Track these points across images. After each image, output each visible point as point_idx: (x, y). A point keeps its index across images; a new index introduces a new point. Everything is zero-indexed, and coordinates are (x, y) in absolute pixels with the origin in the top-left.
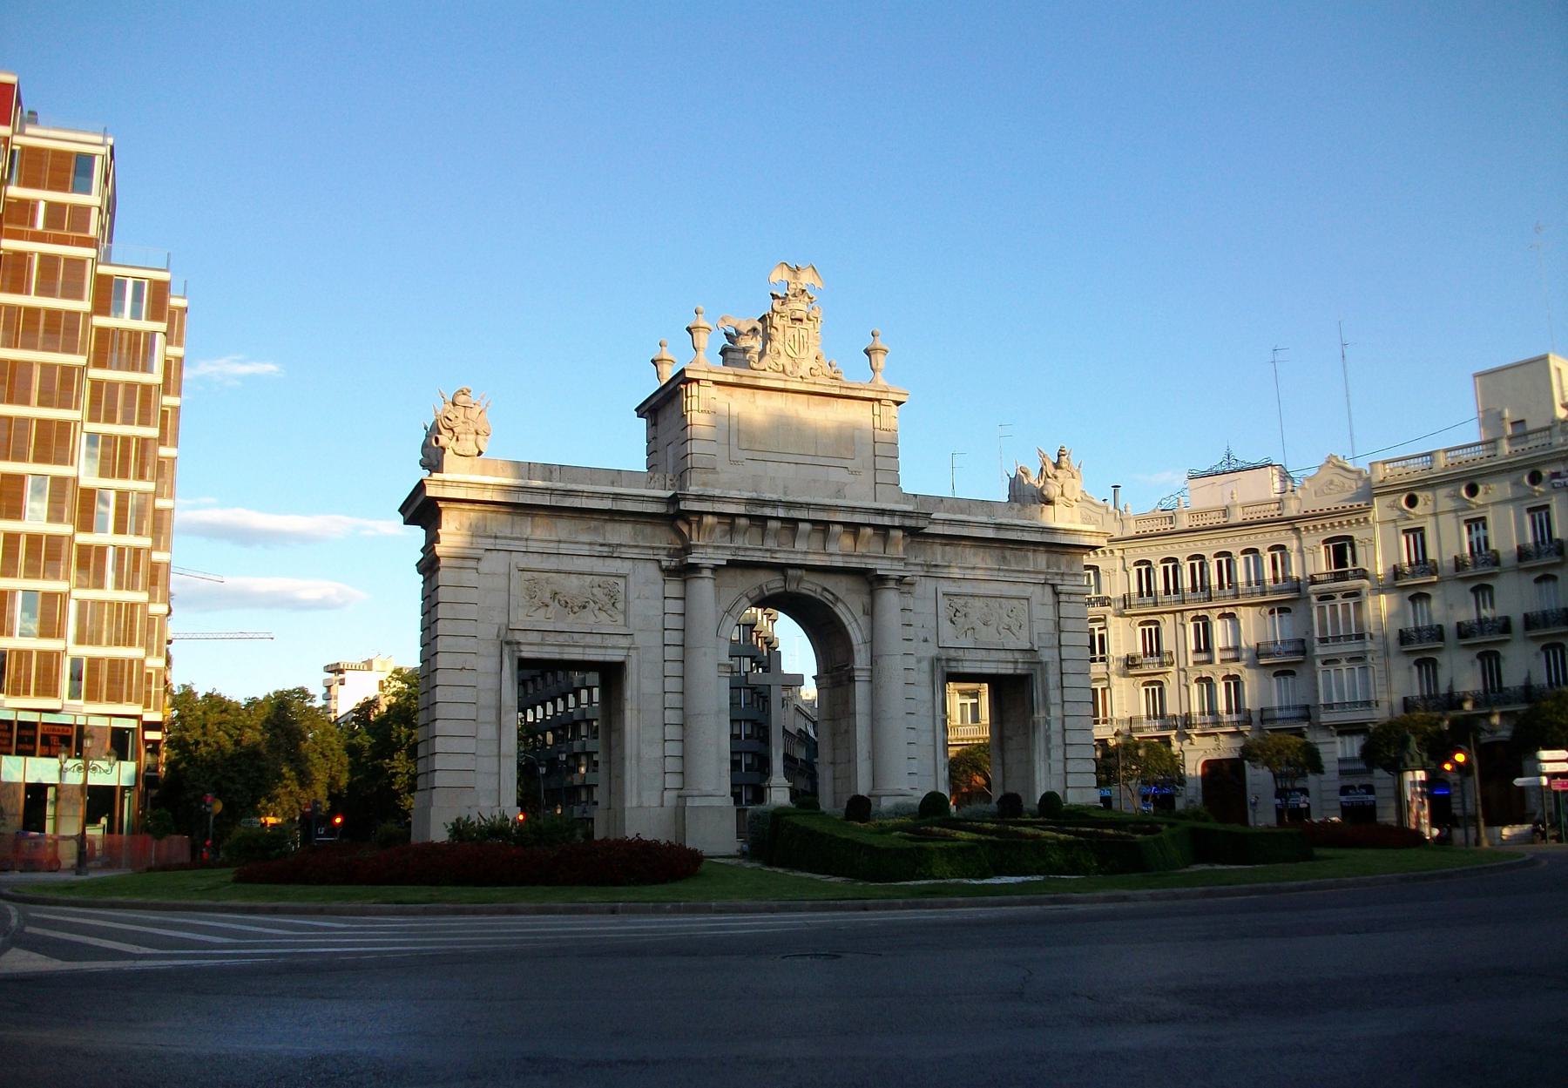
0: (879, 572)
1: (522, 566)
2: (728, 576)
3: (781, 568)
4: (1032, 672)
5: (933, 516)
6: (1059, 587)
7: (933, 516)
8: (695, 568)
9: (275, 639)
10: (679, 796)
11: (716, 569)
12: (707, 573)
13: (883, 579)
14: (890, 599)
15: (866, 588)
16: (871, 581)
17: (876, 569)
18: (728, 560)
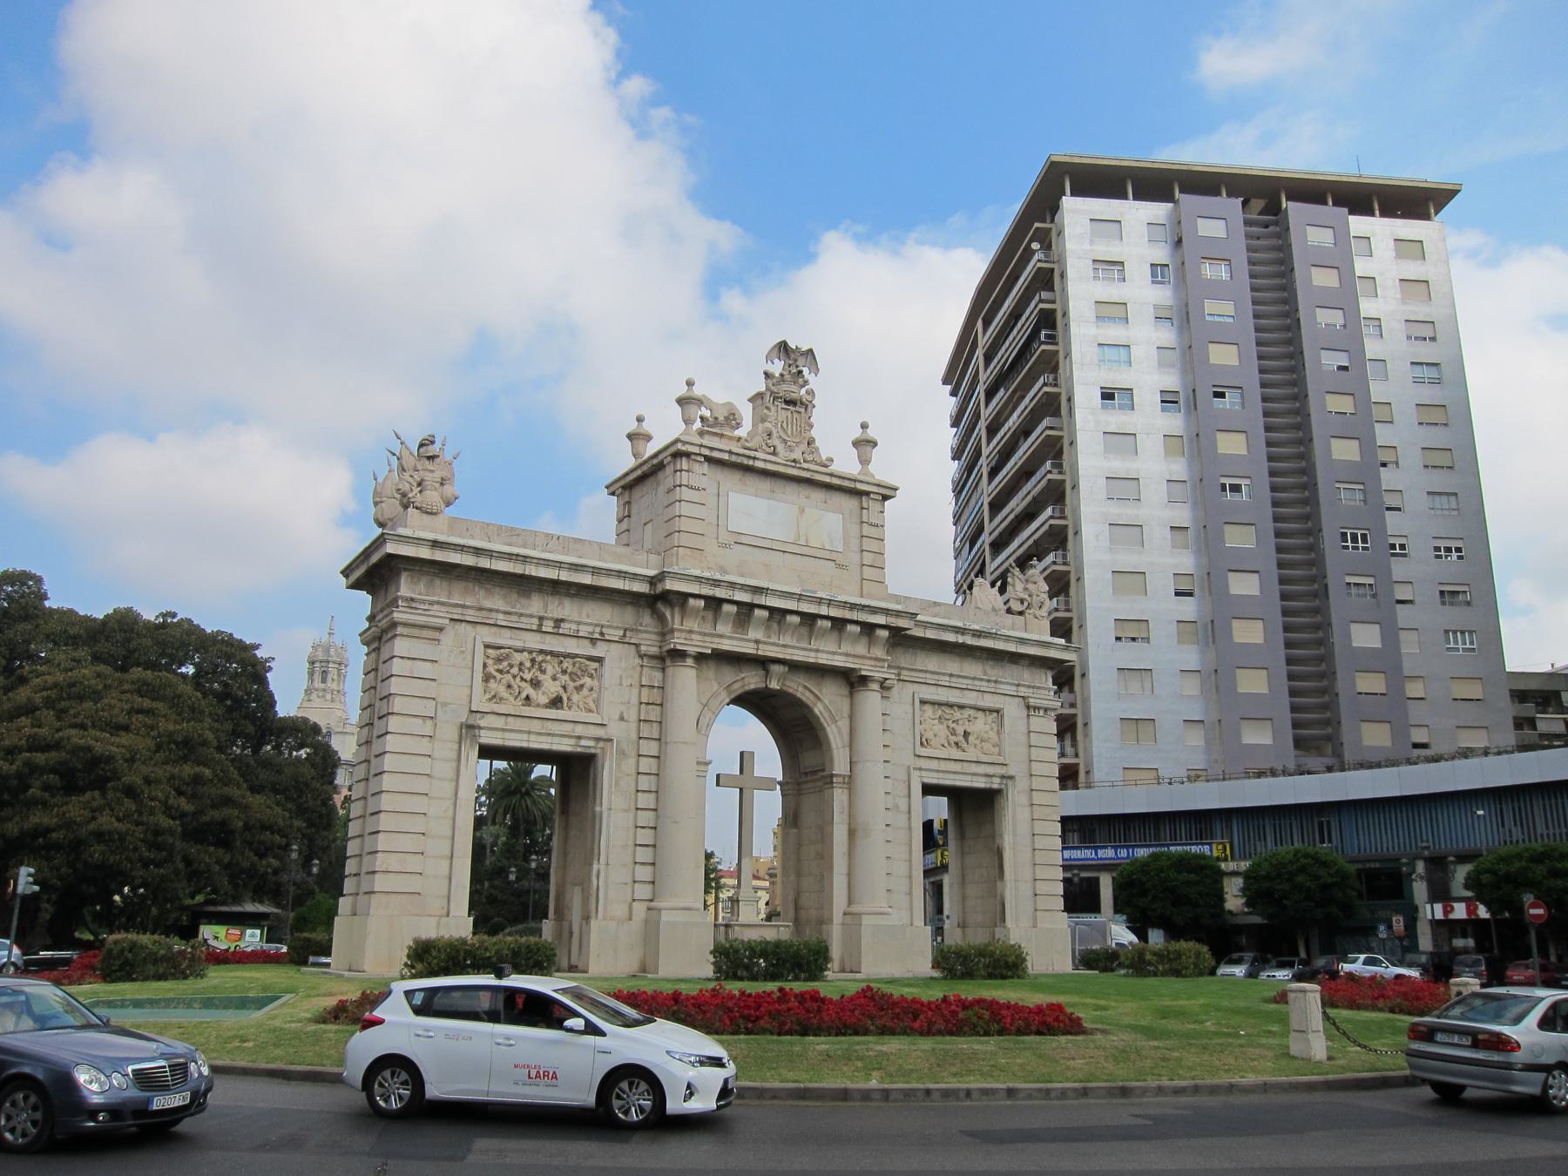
0: (863, 673)
1: (489, 640)
2: (710, 671)
3: (763, 663)
4: (1003, 786)
5: (919, 618)
6: (1031, 700)
7: (919, 618)
8: (678, 655)
9: (641, 413)
10: (649, 909)
11: (700, 658)
12: (690, 662)
13: (864, 680)
14: (871, 699)
15: (845, 691)
16: (853, 681)
17: (860, 669)
18: (713, 650)
